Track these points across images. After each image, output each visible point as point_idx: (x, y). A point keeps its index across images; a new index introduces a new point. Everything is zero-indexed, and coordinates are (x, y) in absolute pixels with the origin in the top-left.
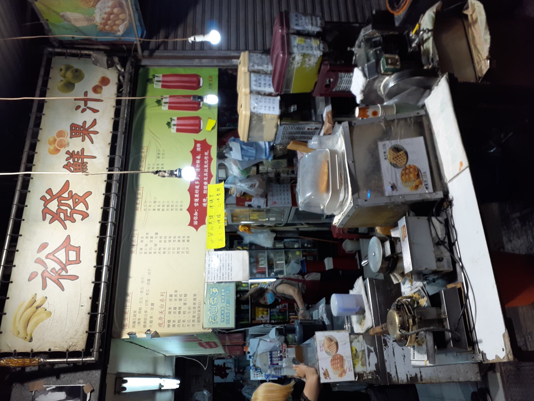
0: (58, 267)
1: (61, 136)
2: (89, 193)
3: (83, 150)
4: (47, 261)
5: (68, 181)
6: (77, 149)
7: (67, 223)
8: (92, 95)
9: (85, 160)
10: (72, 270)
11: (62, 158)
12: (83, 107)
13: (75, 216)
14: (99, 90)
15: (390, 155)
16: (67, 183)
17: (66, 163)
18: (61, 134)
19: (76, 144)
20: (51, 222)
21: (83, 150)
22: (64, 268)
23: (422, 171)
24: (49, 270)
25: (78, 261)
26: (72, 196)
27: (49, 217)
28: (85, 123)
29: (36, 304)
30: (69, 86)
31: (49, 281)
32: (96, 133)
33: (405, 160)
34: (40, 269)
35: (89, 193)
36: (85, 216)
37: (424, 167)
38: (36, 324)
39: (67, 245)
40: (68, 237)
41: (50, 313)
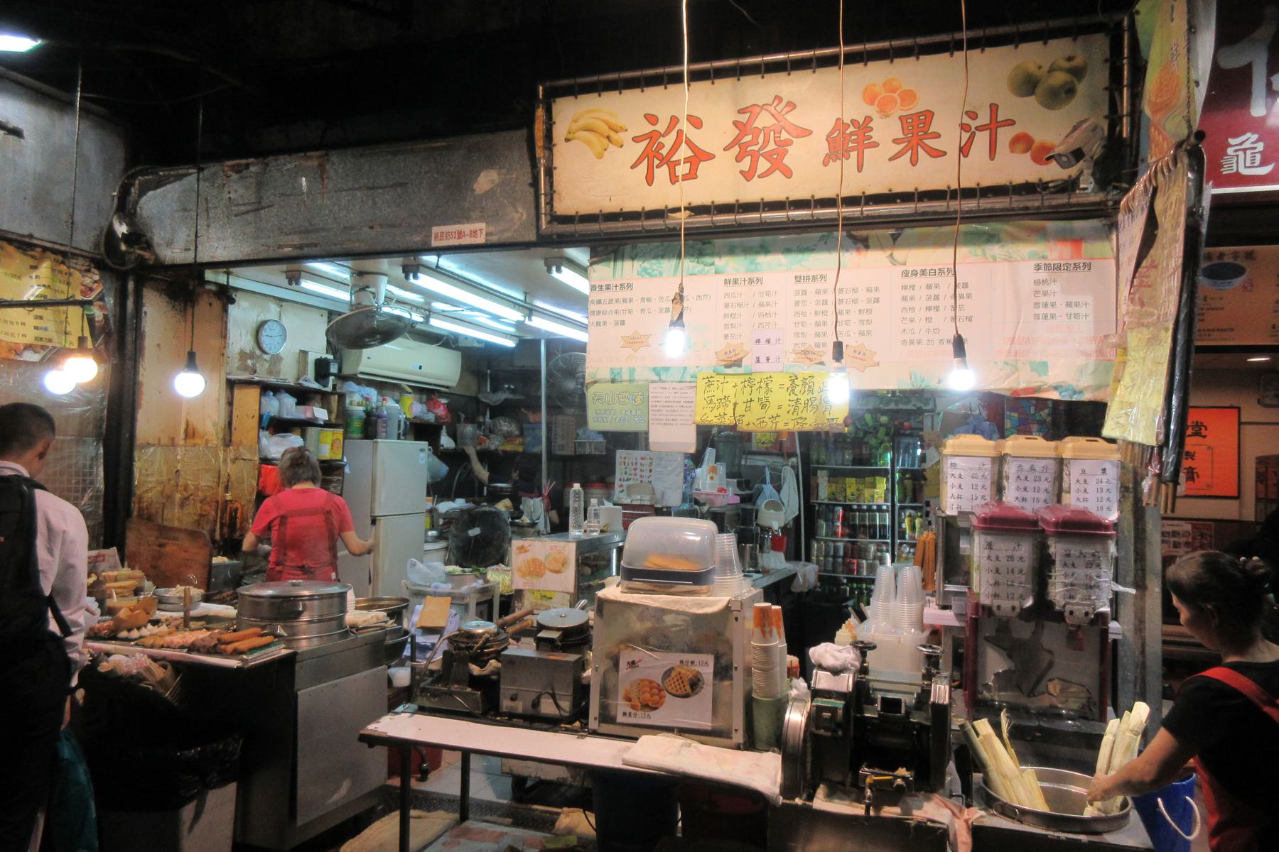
0: (664, 152)
1: (903, 100)
2: (788, 173)
3: (875, 145)
4: (673, 135)
5: (810, 133)
6: (875, 135)
7: (736, 149)
8: (1005, 135)
9: (854, 154)
10: (662, 173)
11: (856, 110)
12: (974, 124)
13: (748, 160)
14: (1020, 146)
15: (688, 672)
16: (807, 133)
17: (847, 121)
18: (909, 97)
19: (887, 130)
20: (735, 123)
21: (875, 145)
22: (665, 160)
23: (652, 713)
24: (661, 140)
25: (674, 179)
26: (783, 145)
27: (744, 118)
28: (937, 136)
29: (612, 134)
30: (1027, 85)
31: (645, 143)
32: (914, 162)
33: (674, 691)
34: (661, 127)
35: (788, 173)
36: (748, 175)
37: (655, 718)
38: (588, 142)
39: (699, 156)
40: (710, 157)
41: (600, 157)
